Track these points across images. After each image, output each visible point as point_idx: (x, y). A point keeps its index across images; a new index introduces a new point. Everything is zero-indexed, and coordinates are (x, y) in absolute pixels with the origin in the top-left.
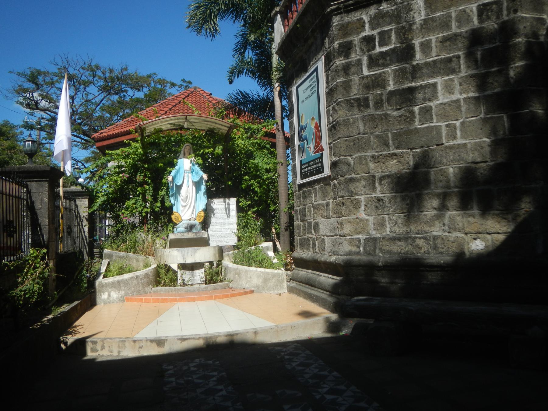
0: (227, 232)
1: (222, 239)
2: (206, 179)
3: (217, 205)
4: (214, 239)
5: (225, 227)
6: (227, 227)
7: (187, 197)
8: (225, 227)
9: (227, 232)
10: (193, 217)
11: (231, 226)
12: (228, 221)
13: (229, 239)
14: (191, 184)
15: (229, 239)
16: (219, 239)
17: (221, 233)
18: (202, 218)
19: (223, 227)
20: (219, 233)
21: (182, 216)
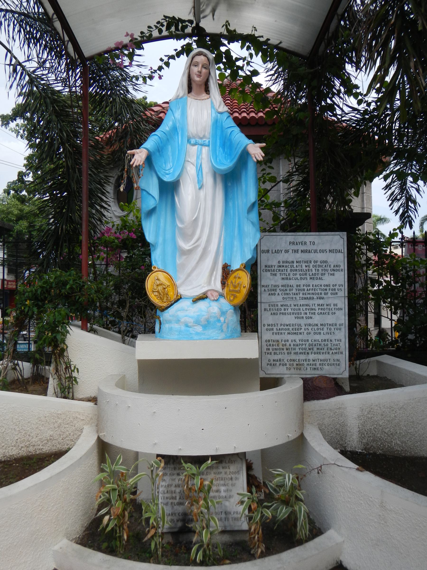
0: (317, 337)
1: (302, 357)
2: (261, 159)
3: (287, 251)
4: (276, 357)
5: (310, 321)
6: (317, 319)
7: (196, 220)
8: (310, 321)
9: (317, 337)
10: (212, 287)
11: (329, 319)
12: (321, 302)
13: (321, 357)
14: (208, 180)
15: (321, 357)
16: (293, 357)
17: (297, 338)
18: (244, 291)
19: (303, 322)
20: (291, 337)
21: (178, 283)
